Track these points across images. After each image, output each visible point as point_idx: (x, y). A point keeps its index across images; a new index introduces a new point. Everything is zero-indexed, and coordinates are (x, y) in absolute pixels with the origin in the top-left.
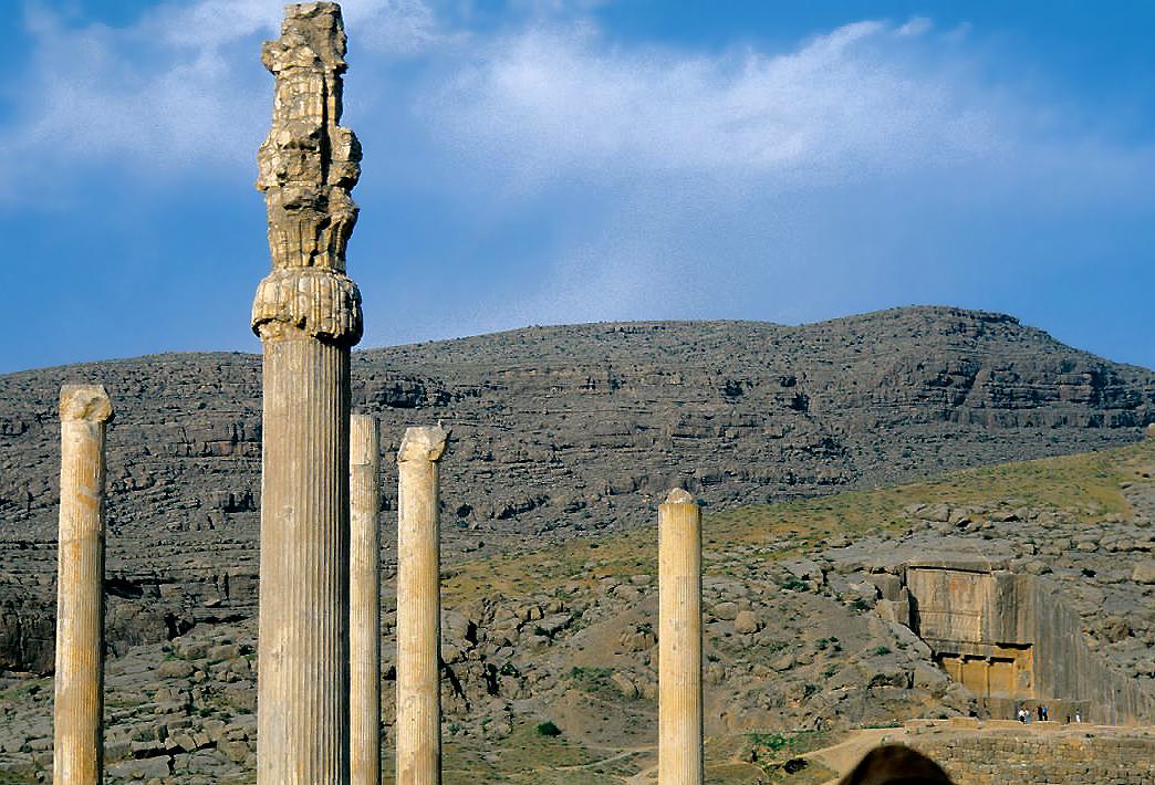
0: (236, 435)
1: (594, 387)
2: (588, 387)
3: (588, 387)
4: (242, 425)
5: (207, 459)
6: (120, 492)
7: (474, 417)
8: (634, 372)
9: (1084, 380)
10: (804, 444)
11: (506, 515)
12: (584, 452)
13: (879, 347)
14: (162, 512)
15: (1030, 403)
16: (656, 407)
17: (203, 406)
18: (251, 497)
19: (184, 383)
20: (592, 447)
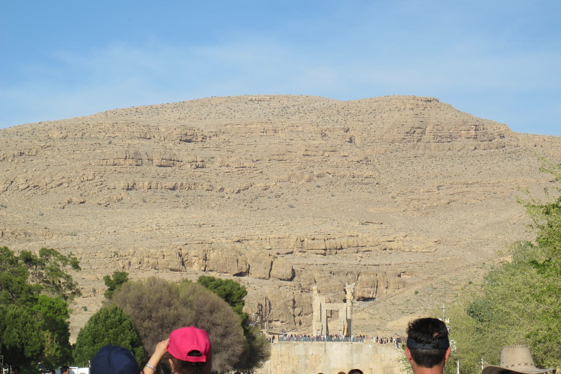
0: (126, 157)
1: (266, 132)
2: (264, 132)
3: (264, 132)
4: (128, 151)
5: (115, 167)
6: (82, 182)
8: (282, 125)
9: (472, 128)
10: (357, 160)
11: (239, 191)
13: (384, 115)
14: (101, 191)
15: (449, 140)
16: (293, 142)
17: (110, 143)
18: (136, 184)
20: (269, 160)
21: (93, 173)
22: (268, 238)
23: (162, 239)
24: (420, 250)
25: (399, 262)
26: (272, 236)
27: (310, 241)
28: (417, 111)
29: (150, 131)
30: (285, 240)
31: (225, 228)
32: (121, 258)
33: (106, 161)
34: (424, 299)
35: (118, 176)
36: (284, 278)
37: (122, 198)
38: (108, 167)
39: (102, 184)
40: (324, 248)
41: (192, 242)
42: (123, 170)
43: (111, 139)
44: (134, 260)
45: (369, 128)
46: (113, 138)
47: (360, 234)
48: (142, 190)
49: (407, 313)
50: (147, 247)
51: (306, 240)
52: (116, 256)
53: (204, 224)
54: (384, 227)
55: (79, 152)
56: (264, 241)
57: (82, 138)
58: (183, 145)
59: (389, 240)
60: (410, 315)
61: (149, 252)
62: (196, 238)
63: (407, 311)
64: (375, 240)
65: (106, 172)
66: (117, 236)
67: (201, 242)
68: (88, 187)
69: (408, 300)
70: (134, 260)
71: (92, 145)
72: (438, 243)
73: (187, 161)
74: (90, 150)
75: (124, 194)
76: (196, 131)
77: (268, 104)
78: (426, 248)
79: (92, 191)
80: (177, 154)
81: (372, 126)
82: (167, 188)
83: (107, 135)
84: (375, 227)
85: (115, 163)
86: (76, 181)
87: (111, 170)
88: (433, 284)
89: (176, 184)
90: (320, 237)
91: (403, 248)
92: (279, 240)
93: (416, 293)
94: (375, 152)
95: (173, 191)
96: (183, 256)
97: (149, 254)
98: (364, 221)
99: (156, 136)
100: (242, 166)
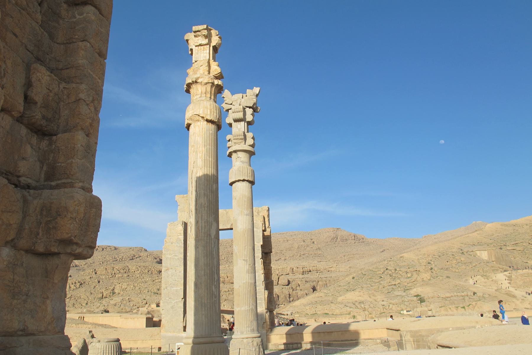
16: (294, 244)
17: (230, 247)
25: (335, 276)
26: (279, 268)
27: (296, 269)
28: (334, 232)
30: (285, 269)
34: (360, 281)
36: (284, 284)
40: (302, 271)
47: (318, 266)
49: (350, 290)
51: (294, 268)
56: (276, 270)
60: (353, 291)
63: (350, 289)
69: (349, 283)
84: (324, 263)
88: (363, 272)
90: (300, 267)
91: (336, 270)
92: (283, 269)
93: (353, 278)
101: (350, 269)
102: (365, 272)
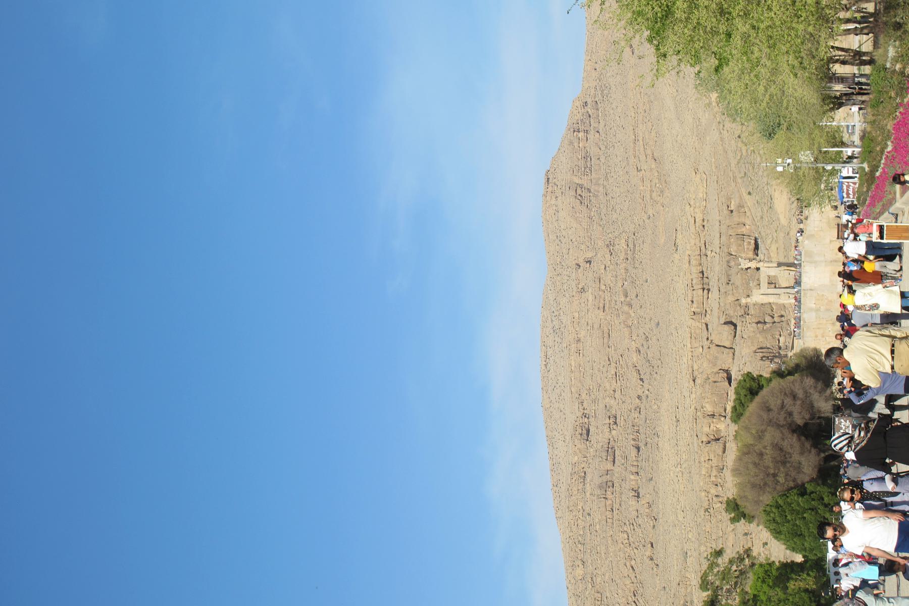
1: (580, 350)
3: (580, 353)
4: (598, 495)
5: (614, 510)
6: (630, 545)
7: (594, 401)
11: (641, 380)
12: (612, 351)
13: (562, 227)
14: (640, 525)
15: (589, 159)
16: (590, 322)
17: (589, 514)
19: (578, 525)
21: (620, 533)
22: (691, 350)
23: (692, 461)
24: (705, 190)
26: (689, 346)
27: (695, 305)
28: (558, 193)
29: (577, 473)
30: (693, 331)
31: (680, 396)
32: (711, 505)
33: (608, 519)
35: (624, 507)
36: (733, 333)
37: (648, 503)
38: (615, 517)
39: (633, 524)
40: (702, 291)
41: (695, 430)
42: (618, 500)
43: (585, 513)
44: (713, 491)
45: (576, 243)
46: (584, 511)
47: (688, 252)
48: (639, 481)
50: (700, 478)
52: (709, 510)
53: (676, 417)
54: (680, 227)
55: (598, 548)
57: (584, 544)
58: (592, 438)
59: (693, 222)
60: (773, 200)
61: (705, 475)
62: (691, 425)
63: (769, 204)
64: (693, 237)
65: (620, 519)
66: (687, 509)
67: (694, 420)
68: (636, 539)
70: (713, 491)
71: (591, 534)
72: (697, 171)
73: (609, 433)
74: (597, 536)
75: (643, 501)
76: (577, 423)
77: (550, 348)
78: (703, 184)
79: (640, 535)
80: (601, 444)
81: (574, 240)
82: (637, 456)
83: (581, 518)
84: (679, 236)
85: (611, 510)
86: (629, 551)
87: (617, 514)
89: (633, 446)
92: (693, 338)
93: (749, 193)
94: (601, 236)
95: (641, 449)
96: (709, 439)
97: (707, 475)
98: (674, 248)
99: (583, 466)
100: (615, 376)
101: (701, 170)
102: (740, 173)
